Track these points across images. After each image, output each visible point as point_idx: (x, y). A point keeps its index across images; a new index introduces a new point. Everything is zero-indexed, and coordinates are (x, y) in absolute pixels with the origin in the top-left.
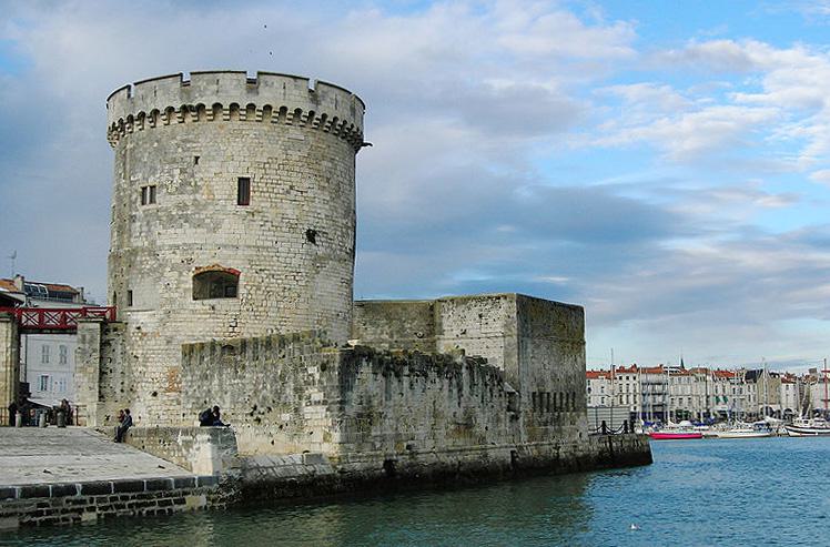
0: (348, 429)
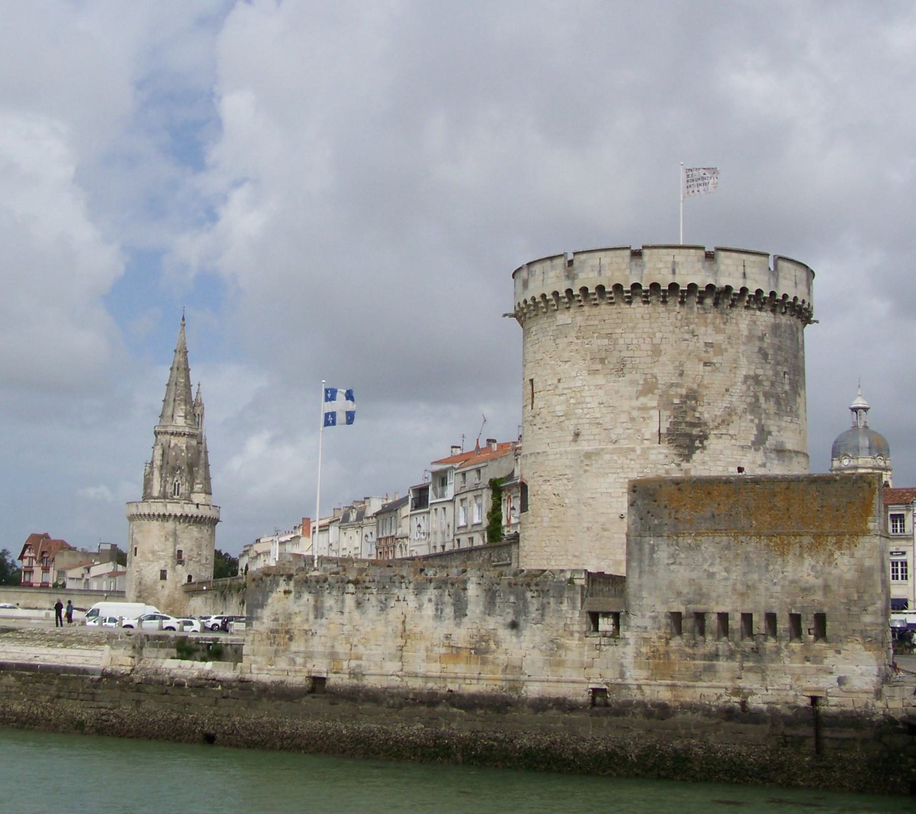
0: (256, 643)
